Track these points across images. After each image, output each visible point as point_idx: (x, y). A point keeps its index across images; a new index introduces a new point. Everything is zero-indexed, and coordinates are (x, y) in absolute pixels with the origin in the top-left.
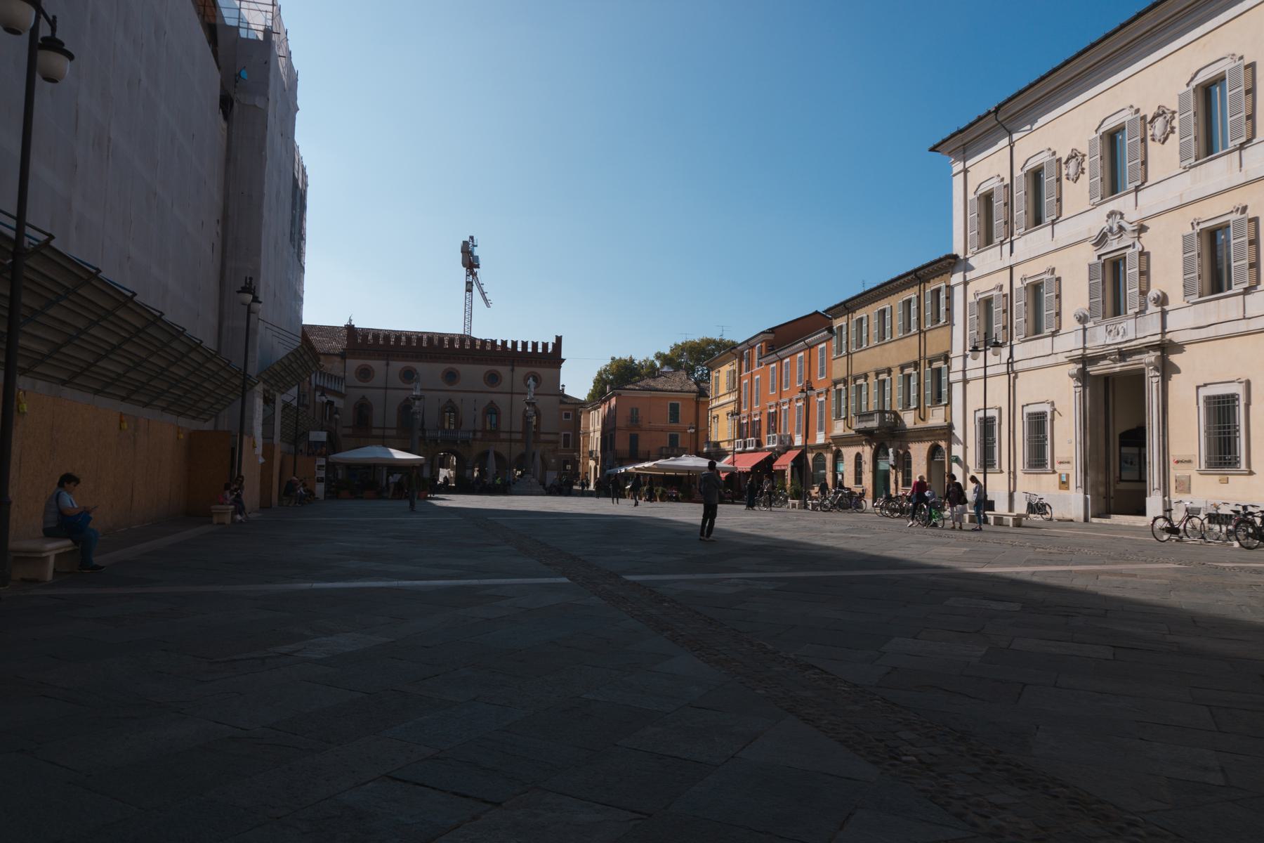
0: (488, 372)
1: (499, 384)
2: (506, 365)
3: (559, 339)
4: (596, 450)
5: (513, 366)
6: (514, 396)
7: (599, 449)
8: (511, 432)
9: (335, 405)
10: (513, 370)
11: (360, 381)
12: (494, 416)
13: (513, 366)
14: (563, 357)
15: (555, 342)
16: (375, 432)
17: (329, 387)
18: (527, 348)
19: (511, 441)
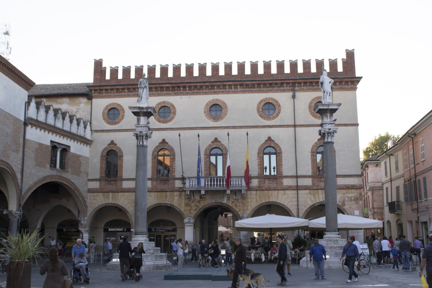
0: (262, 101)
1: (278, 115)
2: (284, 91)
3: (350, 55)
4: (398, 201)
5: (294, 91)
6: (297, 129)
7: (402, 199)
8: (297, 177)
9: (72, 150)
10: (294, 97)
11: (109, 123)
12: (273, 157)
13: (294, 91)
14: (357, 75)
15: (345, 58)
16: (126, 185)
17: (59, 125)
18: (310, 68)
19: (298, 188)
